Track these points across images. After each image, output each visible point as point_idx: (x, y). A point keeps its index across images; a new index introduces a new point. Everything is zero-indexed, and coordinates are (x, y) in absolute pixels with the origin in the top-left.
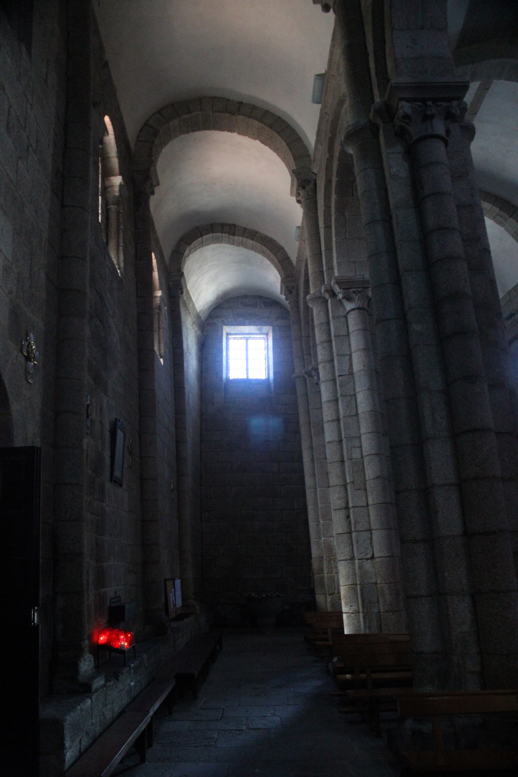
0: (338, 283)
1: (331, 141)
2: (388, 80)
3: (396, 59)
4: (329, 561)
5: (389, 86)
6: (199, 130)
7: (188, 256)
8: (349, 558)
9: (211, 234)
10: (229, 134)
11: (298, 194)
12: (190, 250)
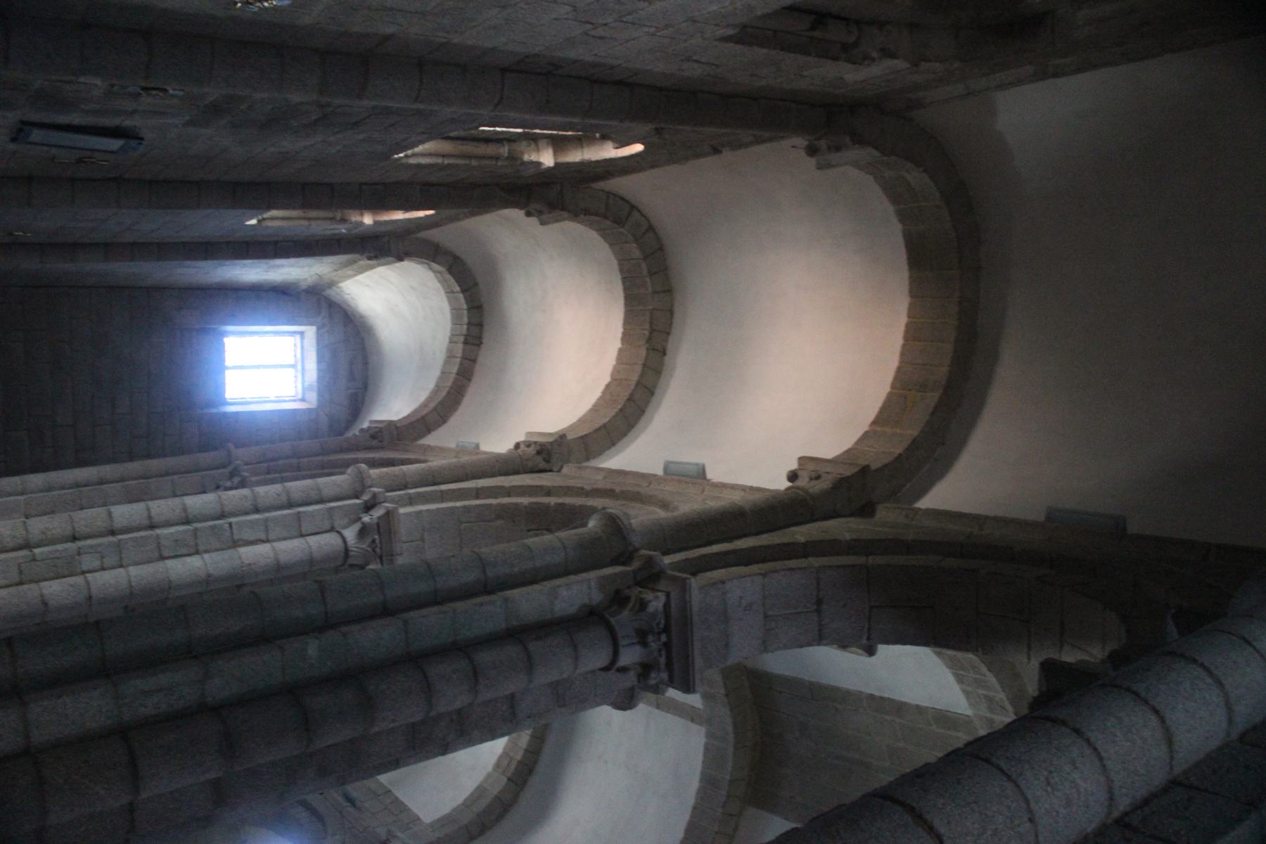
0: (388, 514)
2: (694, 574)
3: (723, 582)
5: (685, 576)
6: (626, 289)
7: (431, 269)
9: (465, 307)
10: (619, 335)
11: (528, 444)
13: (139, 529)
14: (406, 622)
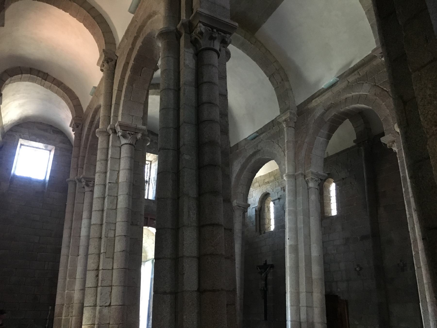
1: (136, 39)
4: (68, 308)
7: (8, 84)
8: (92, 305)
9: (29, 75)
10: (64, 12)
12: (11, 81)
13: (102, 216)
14: (185, 122)
